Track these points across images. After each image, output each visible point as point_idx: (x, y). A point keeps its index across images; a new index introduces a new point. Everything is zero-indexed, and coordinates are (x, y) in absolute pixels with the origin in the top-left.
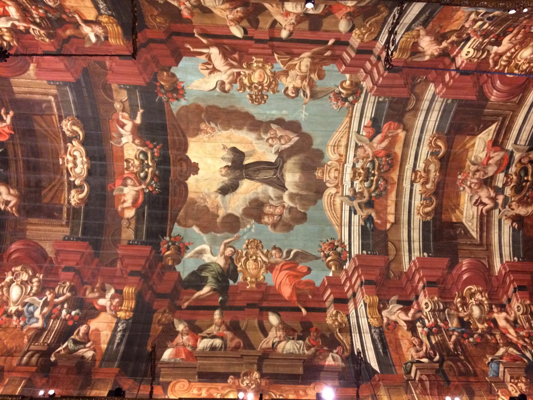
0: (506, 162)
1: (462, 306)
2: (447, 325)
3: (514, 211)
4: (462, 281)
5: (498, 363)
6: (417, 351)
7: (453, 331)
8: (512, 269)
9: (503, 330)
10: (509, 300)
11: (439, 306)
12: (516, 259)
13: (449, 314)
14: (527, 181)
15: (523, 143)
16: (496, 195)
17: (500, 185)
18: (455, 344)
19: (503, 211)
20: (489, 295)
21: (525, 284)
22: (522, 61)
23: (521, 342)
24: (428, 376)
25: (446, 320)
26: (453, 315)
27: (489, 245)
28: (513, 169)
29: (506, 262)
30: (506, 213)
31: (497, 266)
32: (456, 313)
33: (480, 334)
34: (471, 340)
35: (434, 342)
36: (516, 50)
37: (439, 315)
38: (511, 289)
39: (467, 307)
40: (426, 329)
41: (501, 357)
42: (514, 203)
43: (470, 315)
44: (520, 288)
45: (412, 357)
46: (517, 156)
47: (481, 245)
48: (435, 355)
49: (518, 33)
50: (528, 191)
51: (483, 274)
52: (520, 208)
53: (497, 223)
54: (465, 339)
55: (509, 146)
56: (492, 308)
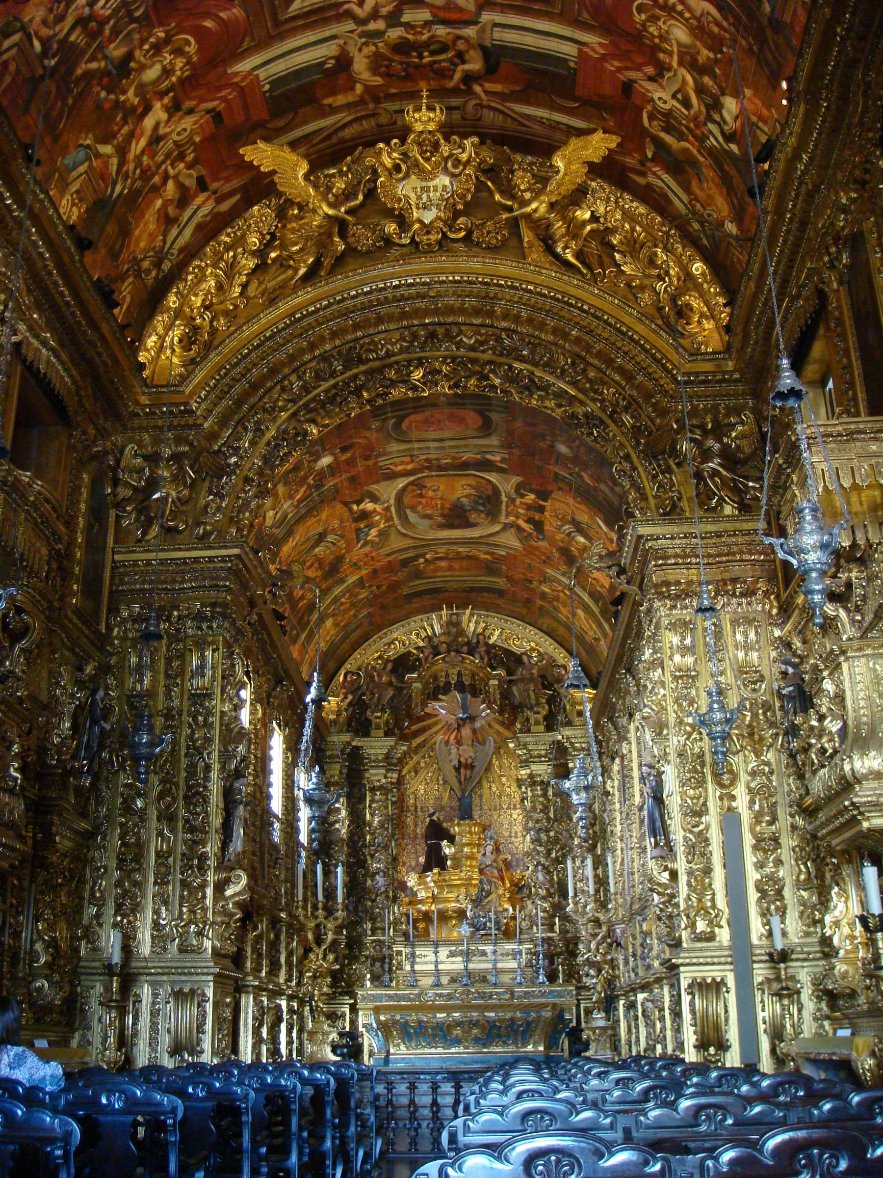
0: (454, 16)
1: (154, 46)
2: (110, 41)
3: (357, 53)
4: (197, 22)
5: (88, 158)
6: (44, 23)
7: (106, 58)
8: (246, 90)
9: (138, 131)
10: (191, 111)
11: (137, 9)
12: (267, 87)
13: (129, 33)
14: (421, 57)
15: (496, 35)
16: (383, 17)
17: (405, 18)
18: (87, 74)
19: (354, 36)
20: (188, 77)
21: (227, 120)
22: (664, 27)
23: (131, 166)
24: (18, 70)
25: (118, 34)
26: (131, 40)
27: (281, 37)
28: (441, 31)
29: (257, 76)
30: (351, 42)
31: (244, 66)
32: (136, 43)
33: (117, 101)
34: (103, 94)
35: (72, 38)
36: (687, 20)
37: (122, 18)
38: (210, 105)
39: (154, 55)
40: (87, 10)
41: (98, 155)
42: (373, 48)
43: (142, 68)
44: (216, 116)
45: (31, 21)
46: (470, 32)
47: (277, 23)
48: (53, 57)
49: (718, 24)
50: (401, 63)
51: (221, 50)
52: (366, 60)
53: (328, 34)
54: (99, 84)
55: (487, 17)
56: (166, 93)
